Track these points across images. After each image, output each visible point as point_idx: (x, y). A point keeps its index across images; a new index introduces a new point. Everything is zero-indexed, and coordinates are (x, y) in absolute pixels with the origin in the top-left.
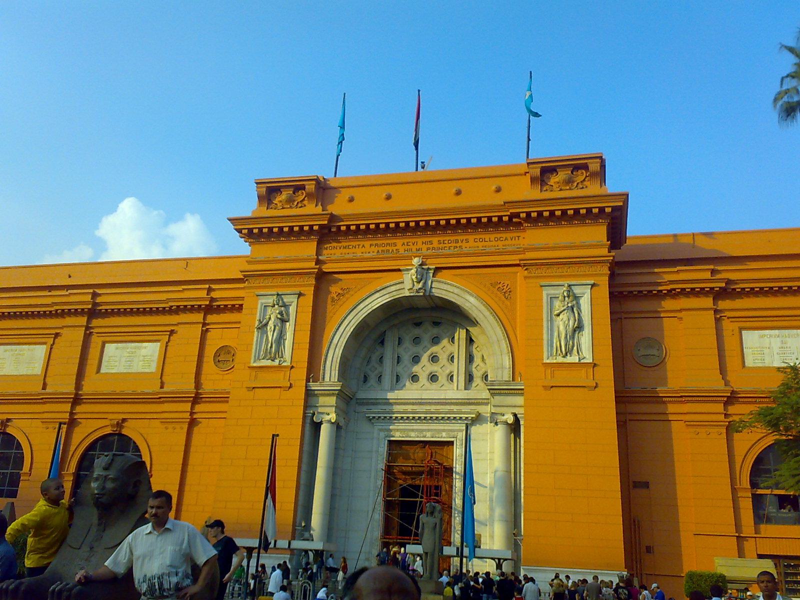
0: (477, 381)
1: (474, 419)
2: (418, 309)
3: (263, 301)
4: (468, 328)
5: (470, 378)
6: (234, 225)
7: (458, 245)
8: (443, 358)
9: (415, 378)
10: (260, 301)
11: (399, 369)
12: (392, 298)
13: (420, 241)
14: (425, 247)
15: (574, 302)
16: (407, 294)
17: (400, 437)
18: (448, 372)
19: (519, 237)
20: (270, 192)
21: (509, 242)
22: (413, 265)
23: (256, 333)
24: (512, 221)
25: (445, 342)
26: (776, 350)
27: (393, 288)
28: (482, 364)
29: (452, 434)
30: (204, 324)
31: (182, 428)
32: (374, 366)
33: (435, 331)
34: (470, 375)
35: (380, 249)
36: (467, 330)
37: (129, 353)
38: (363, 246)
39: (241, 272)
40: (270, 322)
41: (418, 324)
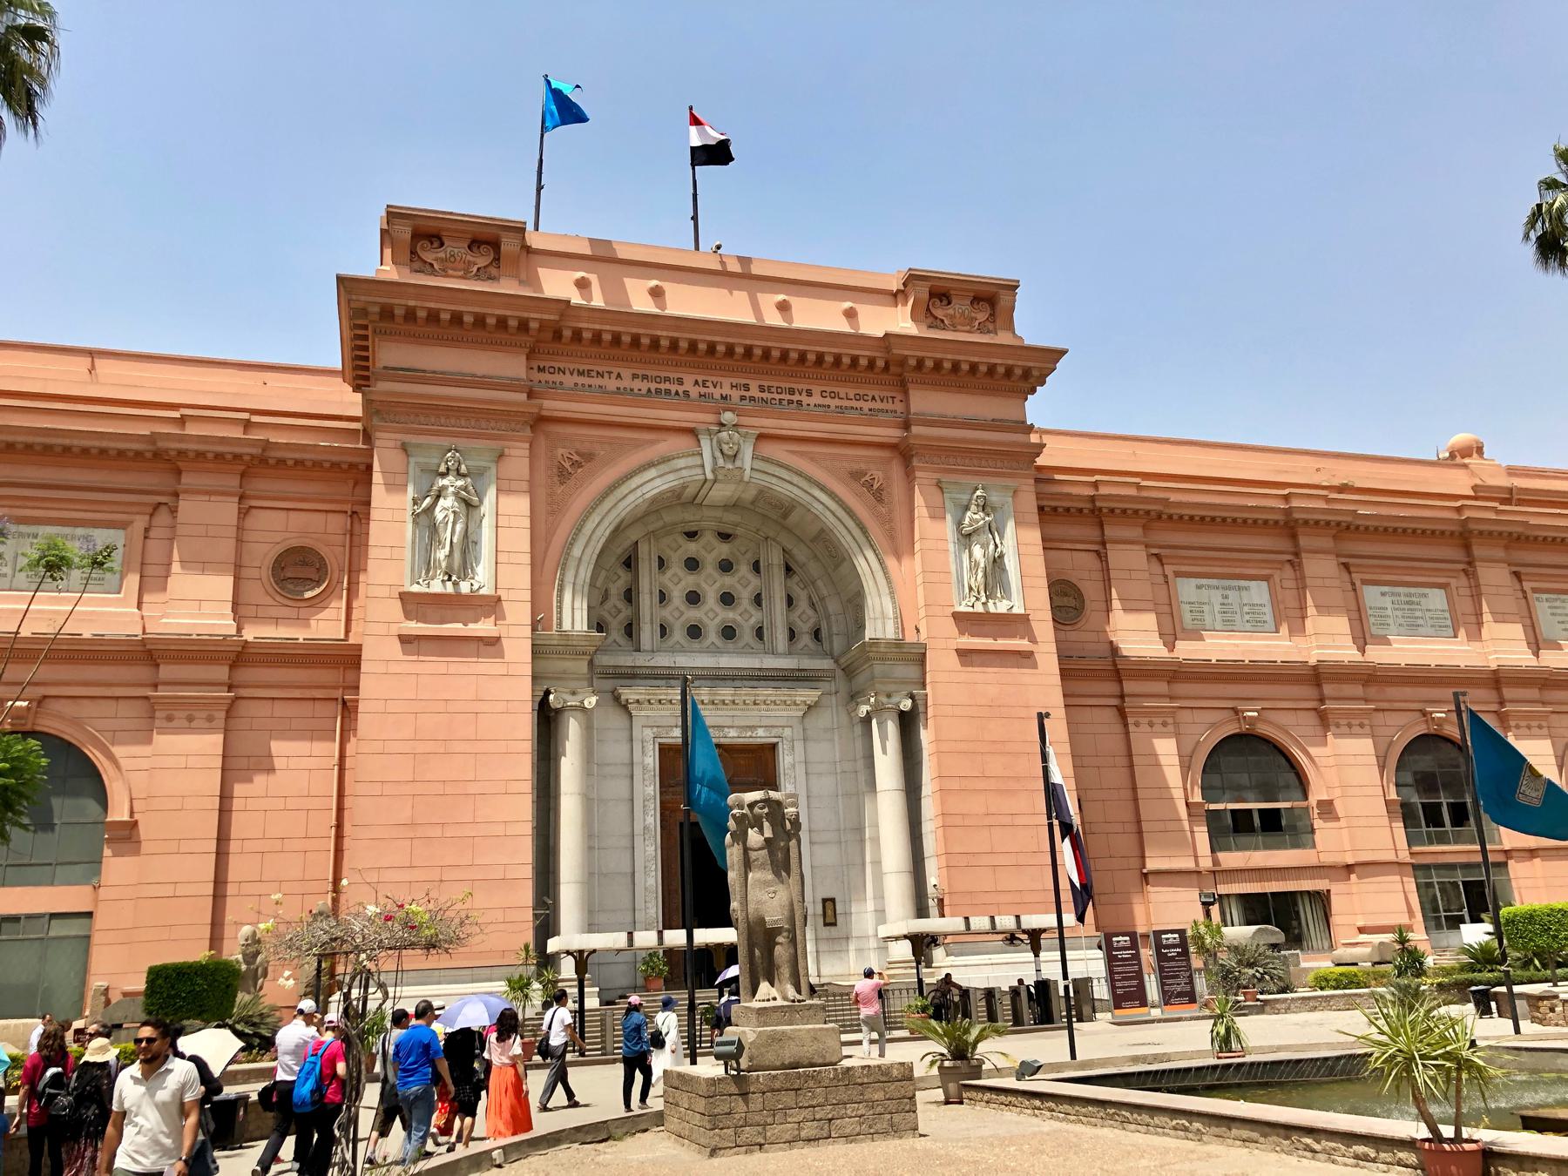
3: (421, 460)
4: (789, 547)
5: (792, 635)
7: (796, 397)
8: (745, 596)
9: (695, 632)
10: (412, 460)
11: (667, 613)
13: (727, 382)
14: (736, 394)
16: (710, 476)
18: (753, 620)
20: (417, 235)
21: (878, 405)
22: (723, 425)
23: (410, 526)
24: (889, 367)
26: (1217, 608)
27: (681, 463)
28: (810, 612)
29: (774, 732)
30: (242, 498)
31: (210, 719)
33: (724, 550)
35: (653, 386)
38: (619, 376)
40: (442, 502)
41: (691, 535)
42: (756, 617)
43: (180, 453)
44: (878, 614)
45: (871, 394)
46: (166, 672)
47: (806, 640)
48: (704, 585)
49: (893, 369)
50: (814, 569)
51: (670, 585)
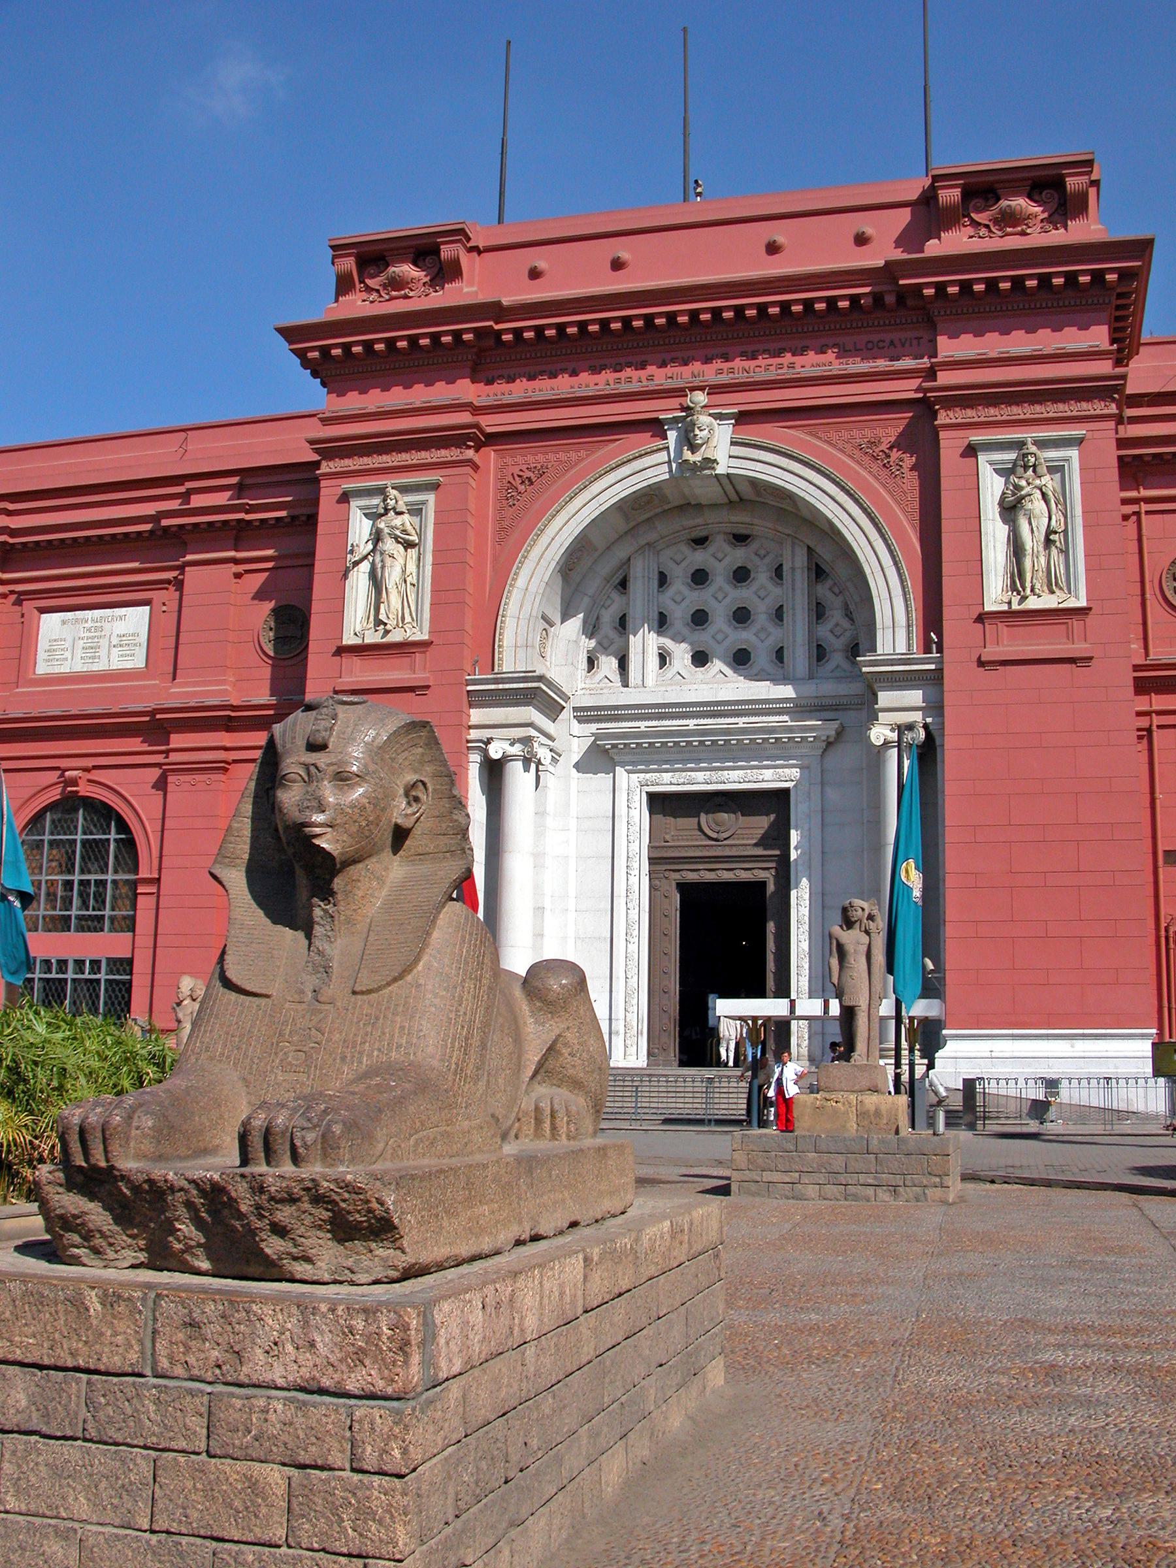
0: (837, 659)
1: (831, 740)
2: (699, 507)
5: (820, 653)
6: (290, 343)
8: (761, 611)
12: (645, 484)
15: (1046, 480)
17: (671, 784)
19: (918, 338)
25: (762, 577)
28: (845, 623)
32: (606, 637)
33: (739, 556)
34: (819, 646)
36: (808, 547)
37: (89, 630)
39: (311, 442)
41: (700, 542)
42: (775, 635)
43: (181, 527)
44: (889, 623)
45: (888, 337)
46: (177, 740)
47: (837, 659)
48: (713, 603)
49: (910, 302)
50: (841, 570)
51: (671, 605)
